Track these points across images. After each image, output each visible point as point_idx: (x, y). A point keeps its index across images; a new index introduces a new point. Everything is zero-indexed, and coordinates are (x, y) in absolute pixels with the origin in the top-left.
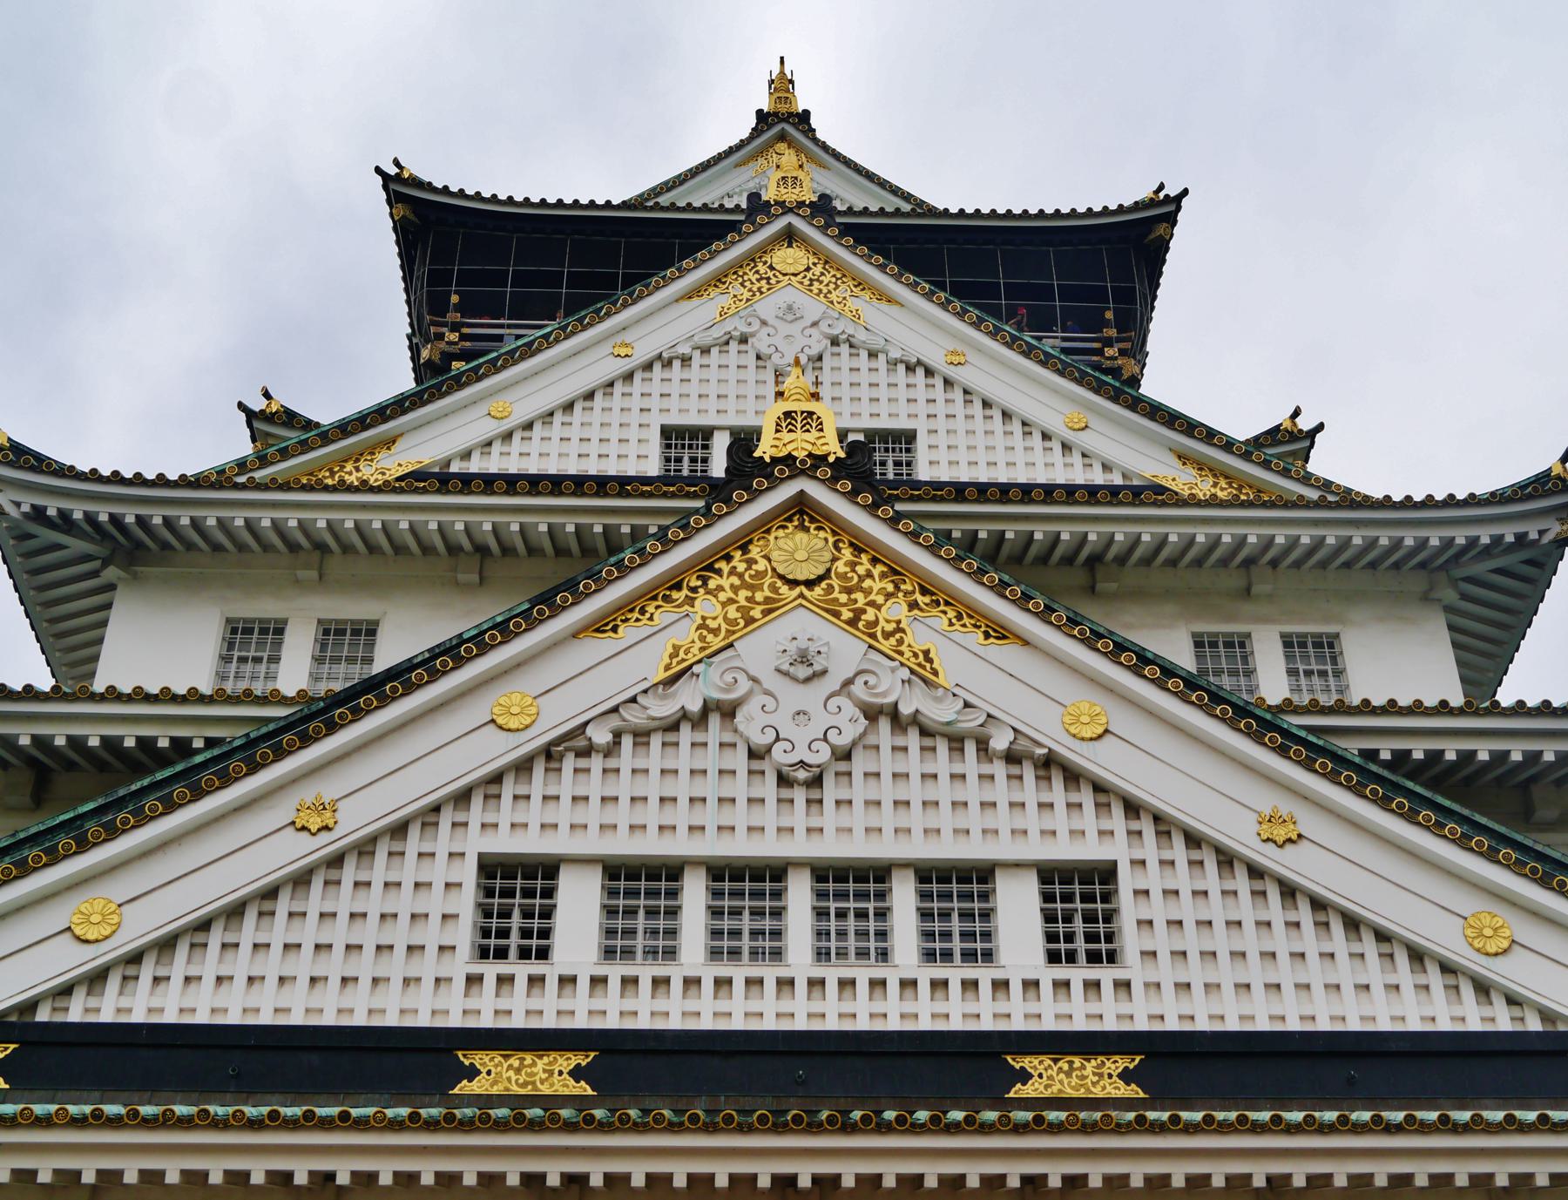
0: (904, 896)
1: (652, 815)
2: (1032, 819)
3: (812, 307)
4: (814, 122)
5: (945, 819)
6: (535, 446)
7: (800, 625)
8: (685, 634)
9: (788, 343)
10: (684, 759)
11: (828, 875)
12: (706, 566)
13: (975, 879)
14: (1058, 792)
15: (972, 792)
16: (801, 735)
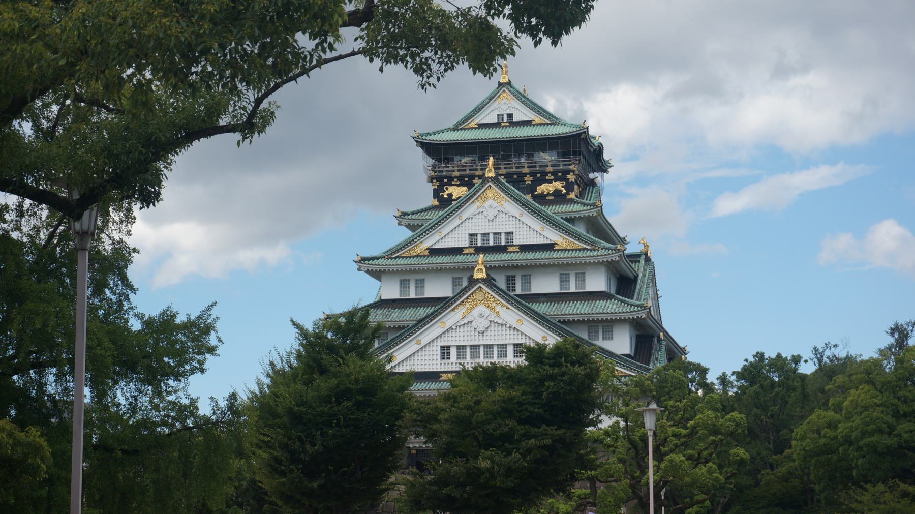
0: (495, 349)
1: (461, 338)
2: (512, 337)
3: (494, 204)
4: (514, 83)
5: (500, 337)
6: (446, 240)
7: (481, 308)
8: (464, 310)
9: (491, 214)
10: (465, 329)
11: (485, 346)
12: (467, 298)
13: (505, 346)
14: (516, 332)
15: (504, 333)
16: (481, 326)
